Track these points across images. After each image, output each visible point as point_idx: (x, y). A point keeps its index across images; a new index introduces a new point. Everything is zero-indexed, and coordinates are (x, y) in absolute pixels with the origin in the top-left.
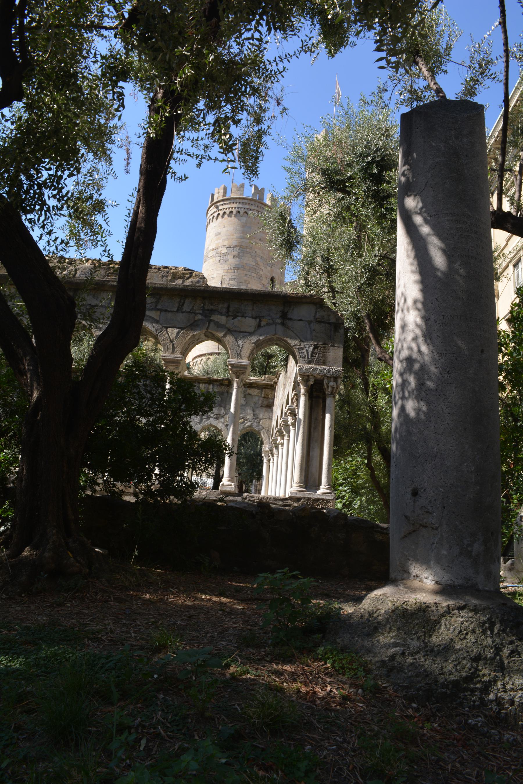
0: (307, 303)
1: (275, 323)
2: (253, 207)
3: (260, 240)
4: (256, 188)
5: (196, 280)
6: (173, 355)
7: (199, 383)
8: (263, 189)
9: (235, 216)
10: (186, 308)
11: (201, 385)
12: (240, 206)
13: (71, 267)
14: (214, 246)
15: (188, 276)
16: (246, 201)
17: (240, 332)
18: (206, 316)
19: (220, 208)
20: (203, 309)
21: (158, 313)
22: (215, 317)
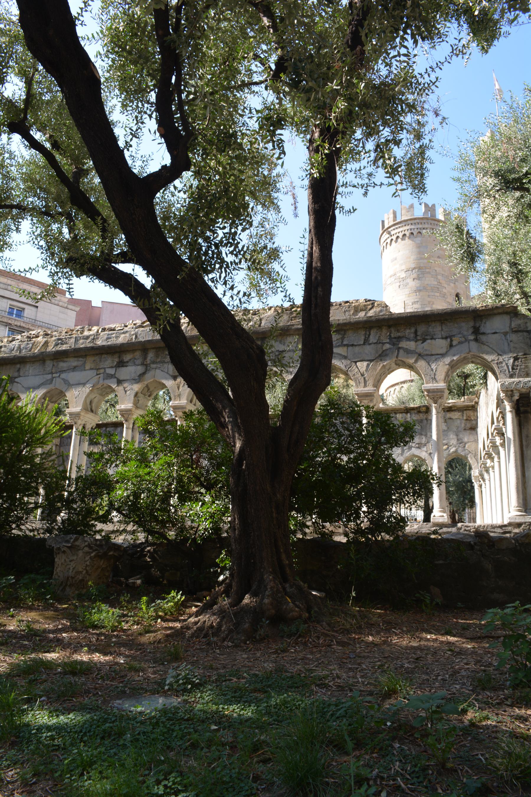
0: (500, 314)
1: (466, 340)
2: (426, 226)
3: (439, 257)
4: (426, 205)
5: (378, 309)
6: (366, 389)
7: (396, 413)
8: (434, 205)
9: (409, 238)
10: (372, 339)
11: (398, 415)
12: (413, 227)
13: (256, 318)
14: (392, 273)
15: (370, 306)
16: (418, 221)
17: (432, 355)
18: (394, 344)
19: (392, 233)
20: (390, 338)
21: (345, 348)
22: (404, 344)
